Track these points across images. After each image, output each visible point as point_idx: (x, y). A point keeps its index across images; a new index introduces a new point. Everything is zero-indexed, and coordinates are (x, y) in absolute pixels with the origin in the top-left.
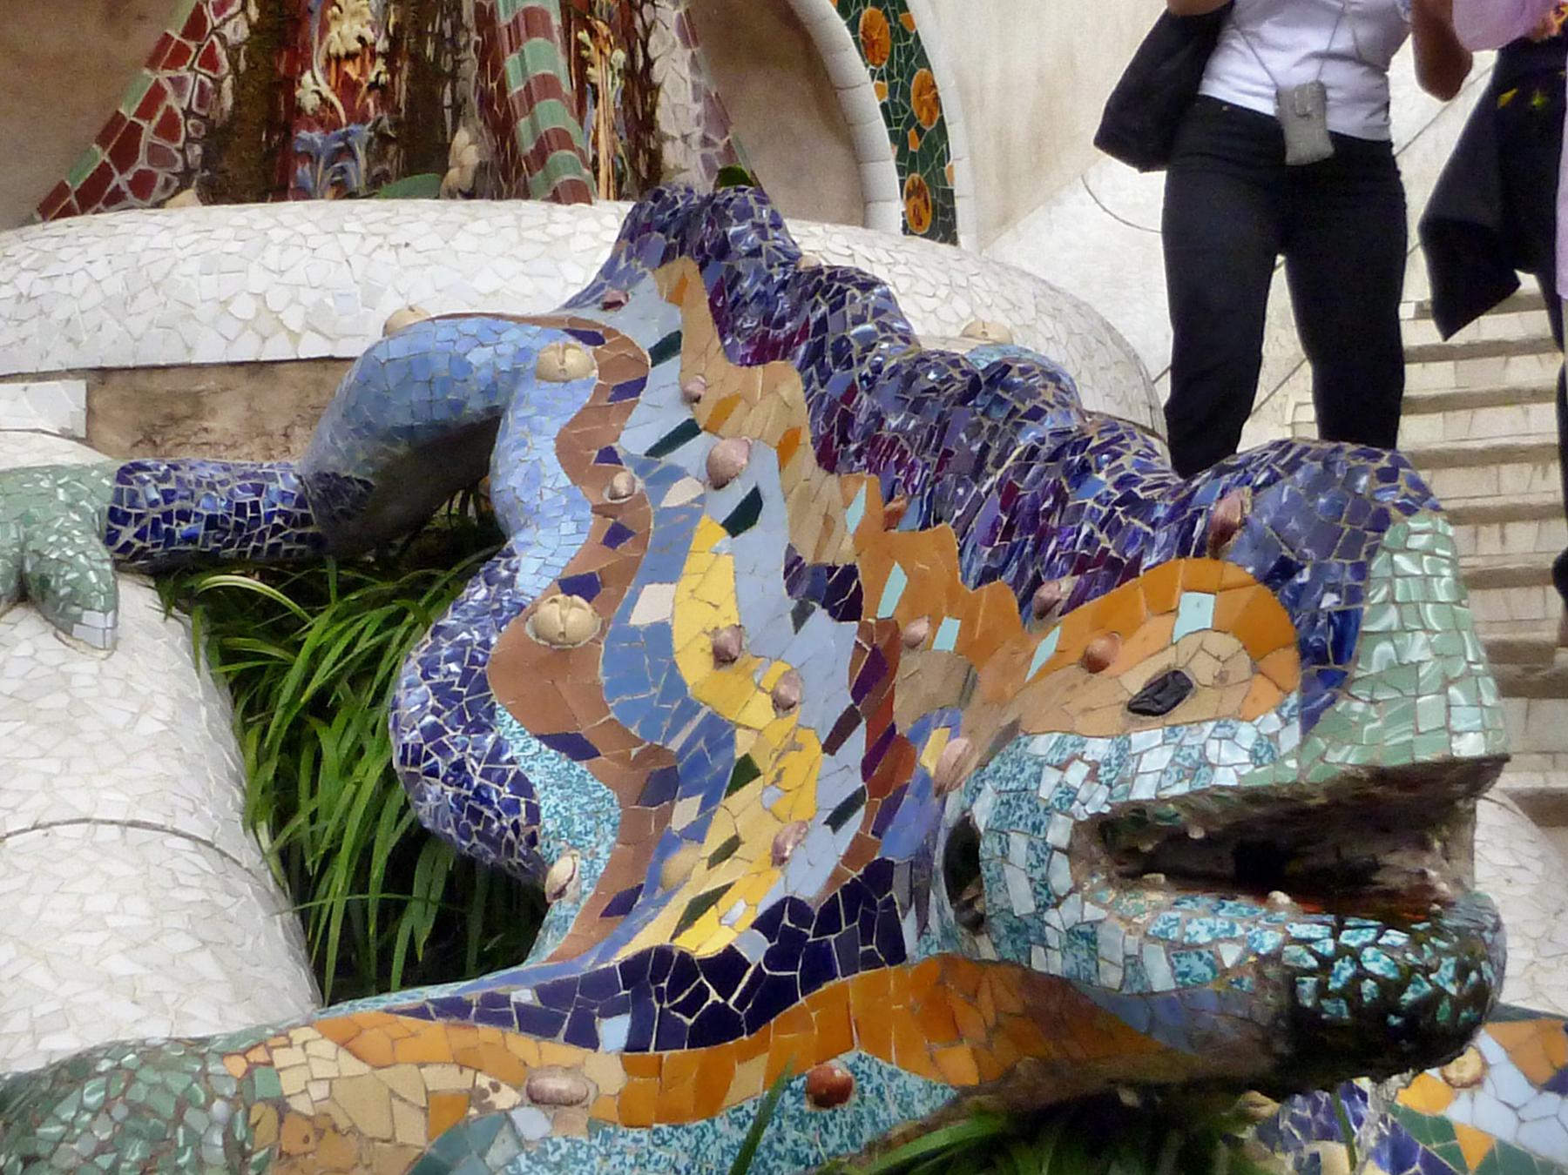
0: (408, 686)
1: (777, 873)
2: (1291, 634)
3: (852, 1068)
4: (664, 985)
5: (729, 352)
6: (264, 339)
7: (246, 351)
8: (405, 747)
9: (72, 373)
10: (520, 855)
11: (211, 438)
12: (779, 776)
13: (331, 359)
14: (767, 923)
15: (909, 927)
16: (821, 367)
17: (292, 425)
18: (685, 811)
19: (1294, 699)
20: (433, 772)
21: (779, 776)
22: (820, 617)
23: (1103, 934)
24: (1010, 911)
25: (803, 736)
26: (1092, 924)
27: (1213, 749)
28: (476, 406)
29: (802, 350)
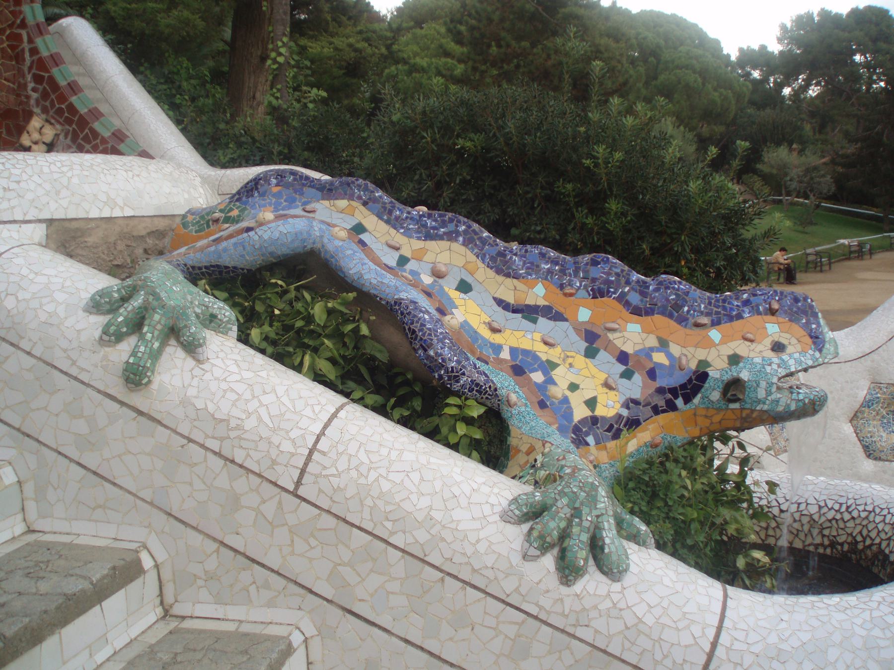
0: (442, 348)
1: (613, 393)
2: (806, 334)
3: (662, 438)
4: (599, 425)
5: (408, 233)
6: (112, 209)
7: (106, 213)
8: (452, 368)
9: (40, 221)
10: (489, 395)
11: (89, 244)
12: (571, 365)
13: (134, 216)
14: (626, 405)
15: (679, 402)
16: (476, 245)
17: (117, 240)
18: (538, 377)
19: (813, 347)
20: (464, 374)
21: (571, 365)
22: (542, 321)
23: (781, 399)
24: (757, 398)
25: (569, 354)
26: (779, 398)
27: (803, 359)
28: (309, 247)
29: (461, 239)
